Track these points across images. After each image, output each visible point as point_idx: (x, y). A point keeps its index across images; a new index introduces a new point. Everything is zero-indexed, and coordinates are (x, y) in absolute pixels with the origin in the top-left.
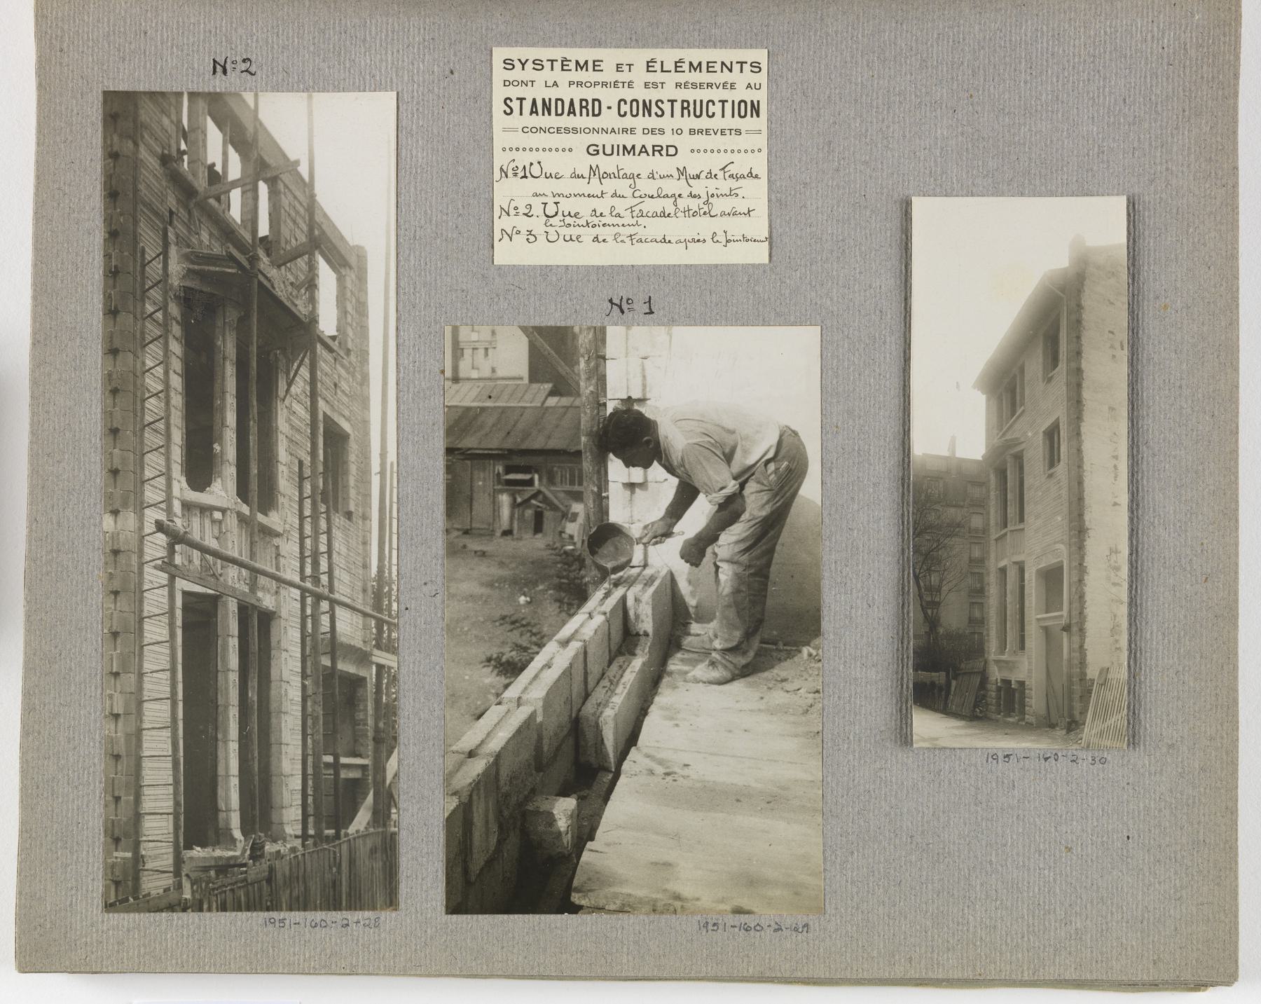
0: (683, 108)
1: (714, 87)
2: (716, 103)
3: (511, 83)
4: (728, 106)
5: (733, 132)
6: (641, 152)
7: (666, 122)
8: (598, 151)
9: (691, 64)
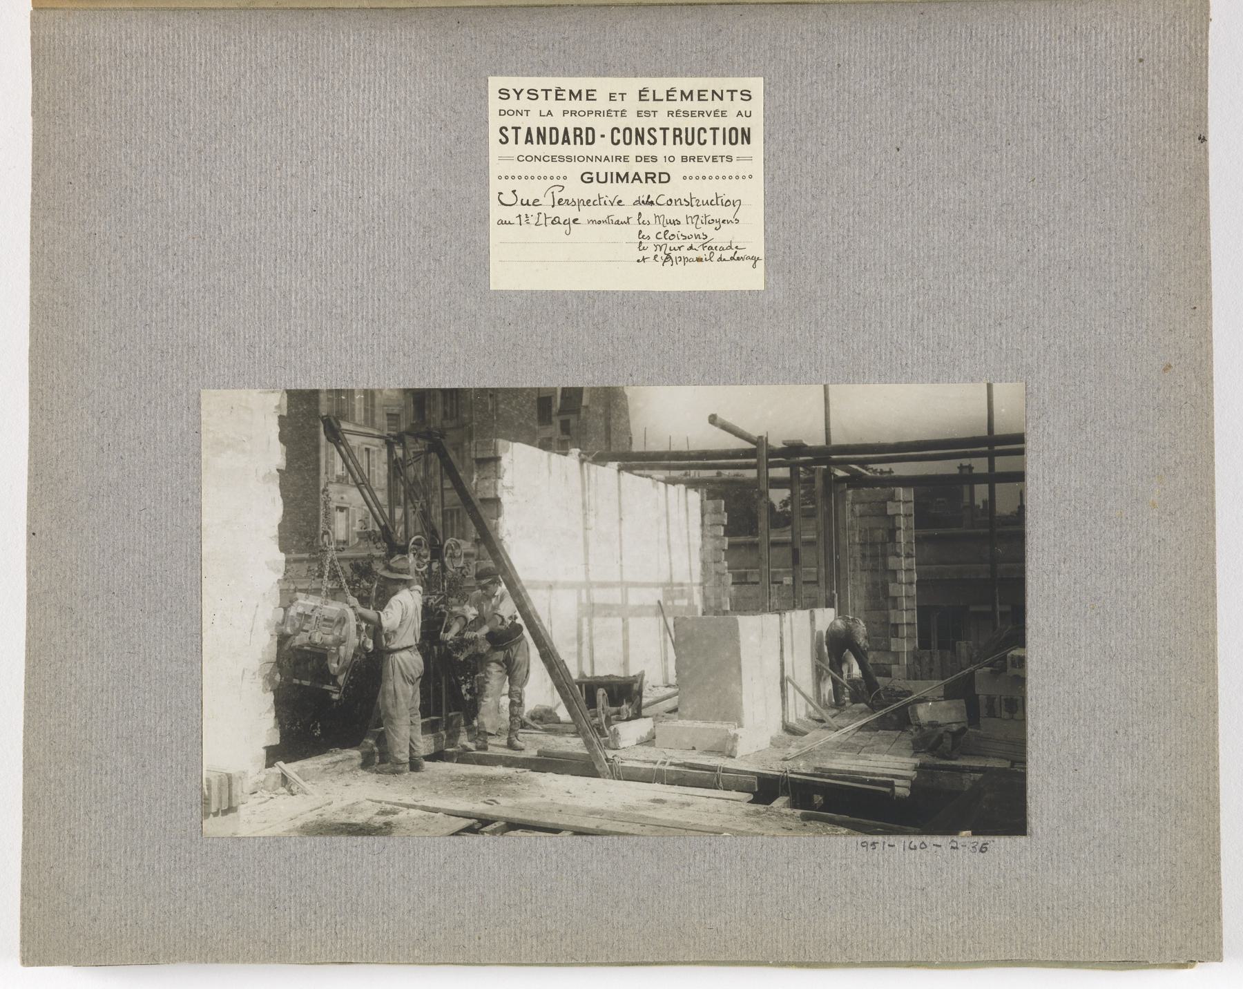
0: (675, 136)
1: (705, 114)
2: (708, 130)
3: (506, 113)
4: (719, 134)
5: (724, 159)
6: (634, 179)
7: (659, 150)
8: (592, 179)
9: (682, 93)
